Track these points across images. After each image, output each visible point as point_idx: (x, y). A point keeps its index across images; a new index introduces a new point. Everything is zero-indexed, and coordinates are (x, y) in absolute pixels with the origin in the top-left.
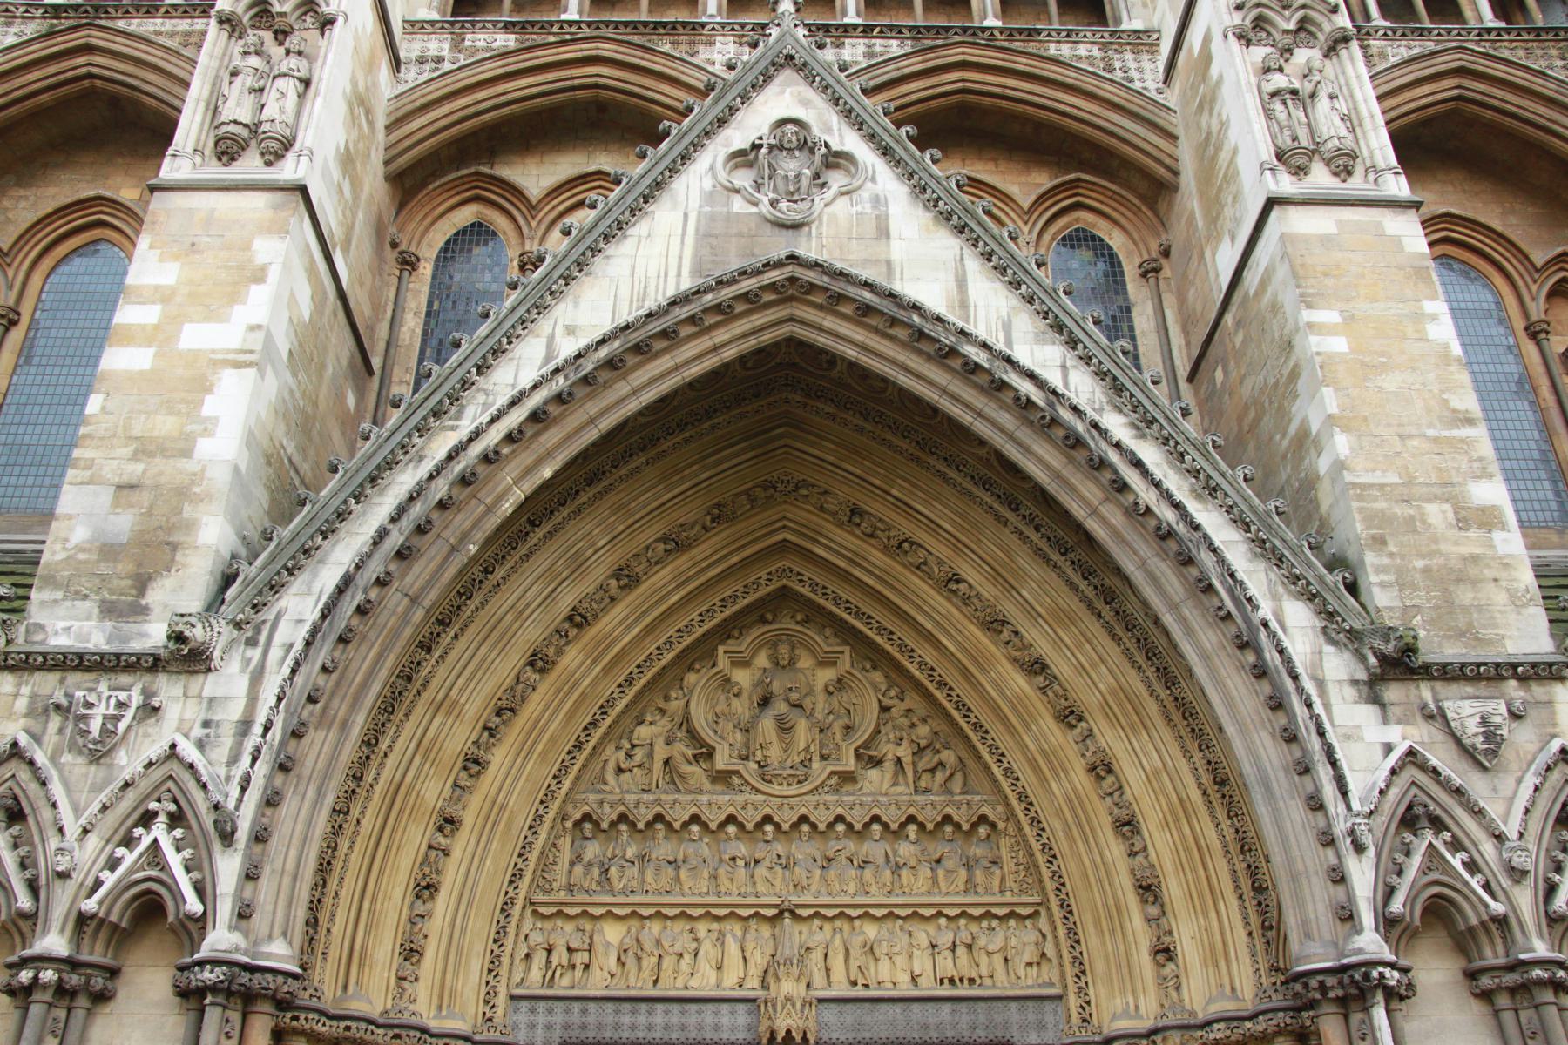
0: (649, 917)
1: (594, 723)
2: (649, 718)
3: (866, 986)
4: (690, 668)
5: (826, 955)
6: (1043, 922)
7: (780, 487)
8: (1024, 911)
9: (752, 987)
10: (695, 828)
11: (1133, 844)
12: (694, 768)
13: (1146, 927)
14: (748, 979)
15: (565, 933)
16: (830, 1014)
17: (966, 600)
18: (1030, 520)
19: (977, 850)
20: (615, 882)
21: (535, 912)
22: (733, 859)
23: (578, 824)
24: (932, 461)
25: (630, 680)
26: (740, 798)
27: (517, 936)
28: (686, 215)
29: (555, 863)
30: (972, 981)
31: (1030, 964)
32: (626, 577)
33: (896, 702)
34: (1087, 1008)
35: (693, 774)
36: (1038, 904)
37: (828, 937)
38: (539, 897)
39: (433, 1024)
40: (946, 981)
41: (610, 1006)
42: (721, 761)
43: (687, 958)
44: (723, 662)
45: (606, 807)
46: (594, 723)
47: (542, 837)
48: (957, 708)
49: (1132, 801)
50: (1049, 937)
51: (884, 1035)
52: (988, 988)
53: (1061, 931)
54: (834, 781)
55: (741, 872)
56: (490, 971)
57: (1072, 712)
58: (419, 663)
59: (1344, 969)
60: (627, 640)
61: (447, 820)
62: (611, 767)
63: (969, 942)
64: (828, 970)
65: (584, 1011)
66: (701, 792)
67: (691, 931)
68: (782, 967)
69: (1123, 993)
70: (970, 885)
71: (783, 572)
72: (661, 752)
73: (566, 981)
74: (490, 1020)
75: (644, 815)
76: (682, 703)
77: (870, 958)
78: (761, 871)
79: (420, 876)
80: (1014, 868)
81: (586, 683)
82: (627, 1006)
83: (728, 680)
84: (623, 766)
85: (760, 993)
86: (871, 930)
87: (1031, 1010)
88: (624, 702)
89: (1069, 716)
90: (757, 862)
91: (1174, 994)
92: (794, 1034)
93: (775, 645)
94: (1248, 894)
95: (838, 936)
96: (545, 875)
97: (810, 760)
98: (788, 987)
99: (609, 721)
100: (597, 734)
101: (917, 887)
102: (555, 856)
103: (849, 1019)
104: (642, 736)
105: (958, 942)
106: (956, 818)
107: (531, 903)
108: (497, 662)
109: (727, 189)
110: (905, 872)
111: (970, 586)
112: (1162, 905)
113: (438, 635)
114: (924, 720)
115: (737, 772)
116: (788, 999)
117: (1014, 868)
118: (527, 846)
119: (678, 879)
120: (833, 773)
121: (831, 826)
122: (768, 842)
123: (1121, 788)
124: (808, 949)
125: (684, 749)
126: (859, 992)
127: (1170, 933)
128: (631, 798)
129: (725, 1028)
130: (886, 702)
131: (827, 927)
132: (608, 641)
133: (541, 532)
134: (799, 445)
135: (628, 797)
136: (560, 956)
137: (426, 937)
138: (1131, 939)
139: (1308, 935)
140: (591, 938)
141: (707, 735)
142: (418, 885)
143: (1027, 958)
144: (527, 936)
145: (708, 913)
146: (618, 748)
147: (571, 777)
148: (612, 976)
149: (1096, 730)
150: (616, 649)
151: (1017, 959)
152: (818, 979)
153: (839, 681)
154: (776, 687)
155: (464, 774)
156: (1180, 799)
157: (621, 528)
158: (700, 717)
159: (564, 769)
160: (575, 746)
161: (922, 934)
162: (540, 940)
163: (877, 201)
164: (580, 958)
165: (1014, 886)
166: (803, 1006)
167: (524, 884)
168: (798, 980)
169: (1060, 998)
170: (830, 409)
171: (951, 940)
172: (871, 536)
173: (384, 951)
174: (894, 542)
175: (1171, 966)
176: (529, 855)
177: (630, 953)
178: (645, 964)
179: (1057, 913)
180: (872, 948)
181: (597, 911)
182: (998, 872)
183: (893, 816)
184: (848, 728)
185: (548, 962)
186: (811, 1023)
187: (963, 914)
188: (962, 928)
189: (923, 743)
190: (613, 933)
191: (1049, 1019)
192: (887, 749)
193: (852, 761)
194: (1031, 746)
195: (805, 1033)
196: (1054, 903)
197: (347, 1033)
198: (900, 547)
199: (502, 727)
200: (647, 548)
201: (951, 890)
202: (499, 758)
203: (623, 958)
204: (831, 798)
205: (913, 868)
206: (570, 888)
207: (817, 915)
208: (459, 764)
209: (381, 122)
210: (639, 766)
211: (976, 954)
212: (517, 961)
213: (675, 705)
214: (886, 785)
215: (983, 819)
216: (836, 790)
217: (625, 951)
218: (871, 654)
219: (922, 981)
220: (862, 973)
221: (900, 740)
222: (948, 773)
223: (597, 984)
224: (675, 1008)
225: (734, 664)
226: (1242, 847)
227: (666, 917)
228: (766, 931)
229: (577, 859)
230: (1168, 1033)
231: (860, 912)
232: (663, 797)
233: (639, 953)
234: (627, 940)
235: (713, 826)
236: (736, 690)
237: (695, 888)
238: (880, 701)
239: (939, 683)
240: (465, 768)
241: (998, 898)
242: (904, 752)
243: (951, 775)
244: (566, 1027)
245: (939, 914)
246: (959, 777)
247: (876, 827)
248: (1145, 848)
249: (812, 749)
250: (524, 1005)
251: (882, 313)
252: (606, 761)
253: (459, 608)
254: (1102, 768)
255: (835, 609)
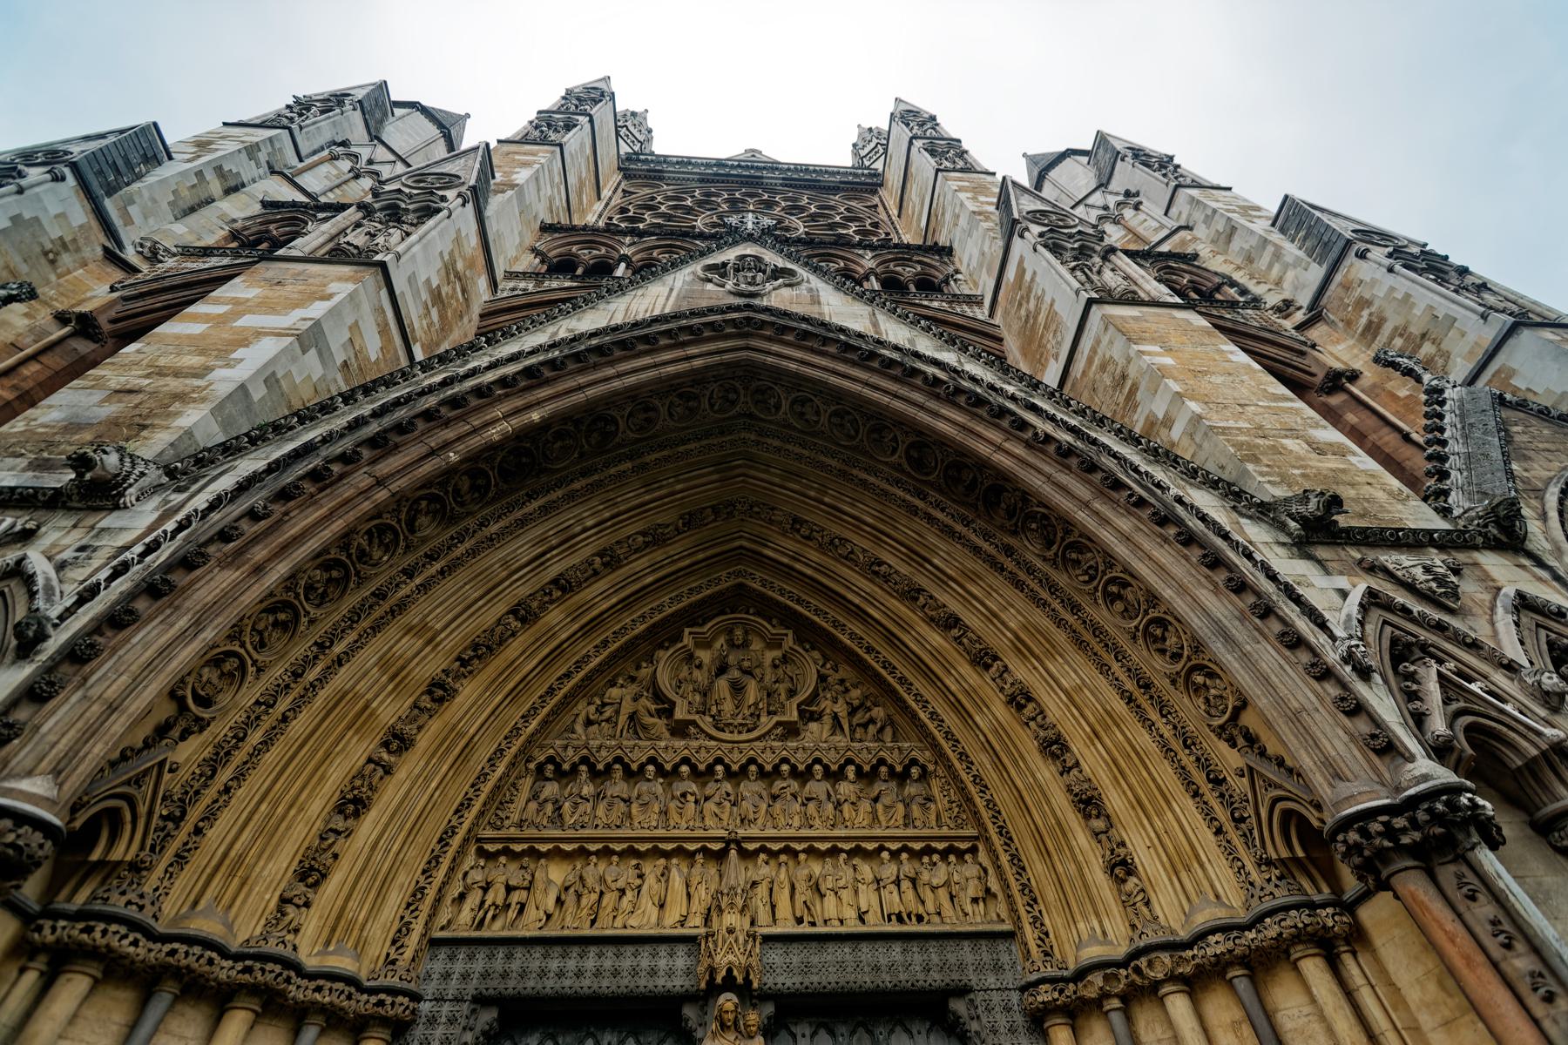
0: (597, 853)
1: (568, 675)
2: (621, 681)
3: (813, 924)
4: (661, 646)
5: (771, 890)
6: (983, 856)
7: (739, 506)
8: (963, 846)
9: (695, 927)
10: (651, 768)
11: (1065, 761)
12: (655, 720)
13: (1094, 843)
14: (691, 915)
15: (507, 872)
16: (776, 956)
17: (886, 578)
18: (937, 505)
19: (911, 789)
20: (567, 818)
21: (481, 853)
22: (684, 795)
23: (540, 768)
24: (855, 472)
25: (605, 643)
26: (695, 744)
27: (451, 869)
28: (671, 290)
29: (512, 801)
30: (920, 919)
31: (975, 900)
32: (611, 560)
33: (831, 672)
34: (1046, 940)
35: (654, 725)
36: (976, 838)
37: (774, 874)
38: (489, 833)
39: (311, 962)
40: (894, 917)
41: (538, 952)
42: (680, 714)
43: (629, 895)
44: (687, 640)
45: (570, 752)
46: (568, 675)
47: (500, 770)
48: (884, 667)
49: (1055, 722)
50: (991, 871)
51: (833, 978)
52: (936, 924)
53: (1004, 859)
54: (779, 730)
55: (691, 807)
56: (409, 905)
57: (987, 654)
58: (397, 585)
59: (1414, 802)
60: (605, 607)
61: (395, 736)
62: (581, 720)
63: (912, 875)
64: (773, 907)
65: (509, 957)
66: (659, 738)
67: (637, 867)
68: (725, 898)
69: (1086, 918)
70: (908, 820)
71: (738, 574)
72: (627, 708)
73: (498, 924)
74: (393, 962)
75: (604, 757)
76: (650, 670)
77: (817, 898)
78: (710, 806)
79: (349, 788)
80: (947, 806)
81: (564, 636)
82: (558, 950)
83: (690, 658)
84: (592, 717)
85: (702, 931)
86: (816, 868)
87: (984, 948)
88: (598, 660)
89: (983, 659)
90: (707, 799)
91: (1145, 910)
92: (735, 973)
93: (730, 632)
94: (1205, 788)
95: (783, 869)
96: (499, 813)
97: (759, 716)
98: (731, 919)
99: (582, 674)
100: (569, 685)
101: (858, 823)
102: (512, 795)
103: (795, 960)
104: (613, 695)
105: (902, 876)
106: (889, 761)
107: (479, 840)
108: (481, 603)
109: (702, 280)
110: (846, 807)
111: (890, 566)
112: (1108, 817)
113: (424, 566)
114: (855, 686)
115: (694, 723)
116: (731, 931)
117: (947, 806)
118: (483, 776)
119: (630, 816)
120: (778, 724)
121: (776, 768)
122: (717, 781)
123: (1042, 712)
124: (754, 884)
125: (648, 704)
126: (805, 929)
127: (1123, 844)
128: (594, 743)
129: (662, 973)
130: (823, 671)
131: (772, 862)
132: (588, 606)
133: (535, 504)
134: (752, 472)
135: (591, 742)
136: (497, 895)
137: (336, 856)
138: (1080, 858)
139: (1338, 776)
140: (533, 876)
141: (671, 695)
142: (344, 798)
143: (971, 892)
144: (466, 874)
145: (656, 847)
146: (589, 704)
147: (539, 718)
148: (549, 916)
149: (1010, 666)
150: (595, 612)
151: (962, 894)
152: (763, 916)
153: (784, 656)
154: (732, 659)
155: (426, 697)
156: (1106, 710)
157: (607, 515)
158: (665, 681)
159: (534, 710)
160: (547, 693)
161: (866, 870)
162: (479, 878)
163: (810, 290)
164: (516, 897)
165: (949, 821)
166: (746, 942)
167: (470, 816)
168: (742, 912)
169: (1009, 936)
170: (776, 443)
171: (895, 873)
172: (808, 538)
173: (278, 868)
174: (827, 539)
175: (1133, 880)
176: (482, 786)
177: (572, 890)
178: (584, 901)
179: (997, 841)
180: (817, 885)
181: (544, 848)
182: (933, 806)
183: (833, 760)
184: (792, 693)
185: (483, 902)
186: (754, 961)
187: (905, 849)
188: (905, 862)
189: (856, 703)
190: (557, 873)
191: (1005, 958)
192: (826, 705)
193: (795, 713)
194: (953, 688)
195: (748, 974)
196: (993, 831)
197: (170, 959)
198: (831, 545)
199: (476, 662)
200: (629, 537)
201: (891, 826)
202: (468, 691)
203: (563, 897)
204: (776, 744)
205: (853, 803)
206: (520, 825)
207: (763, 849)
208: (423, 688)
209: (476, 310)
210: (607, 720)
211: (920, 890)
212: (448, 900)
213: (645, 671)
214: (825, 735)
215: (914, 762)
216: (783, 738)
217: (567, 889)
218: (810, 635)
219: (869, 918)
220: (809, 909)
221: (835, 701)
222: (879, 725)
223: (530, 926)
224: (610, 951)
225: (698, 645)
226: (1185, 742)
227: (613, 852)
228: (712, 870)
229: (535, 797)
230: (1153, 955)
231: (804, 846)
232: (625, 743)
233: (581, 889)
234: (571, 877)
235: (668, 767)
236: (697, 662)
237: (645, 824)
238: (818, 671)
239: (867, 648)
240: (429, 692)
241: (936, 832)
242: (841, 709)
243: (881, 730)
244: (485, 975)
245: (881, 849)
246: (888, 731)
247: (817, 767)
248: (1077, 764)
249: (761, 706)
250: (443, 953)
251: (816, 336)
252: (577, 715)
253: (449, 548)
254: (1020, 699)
255: (781, 599)
